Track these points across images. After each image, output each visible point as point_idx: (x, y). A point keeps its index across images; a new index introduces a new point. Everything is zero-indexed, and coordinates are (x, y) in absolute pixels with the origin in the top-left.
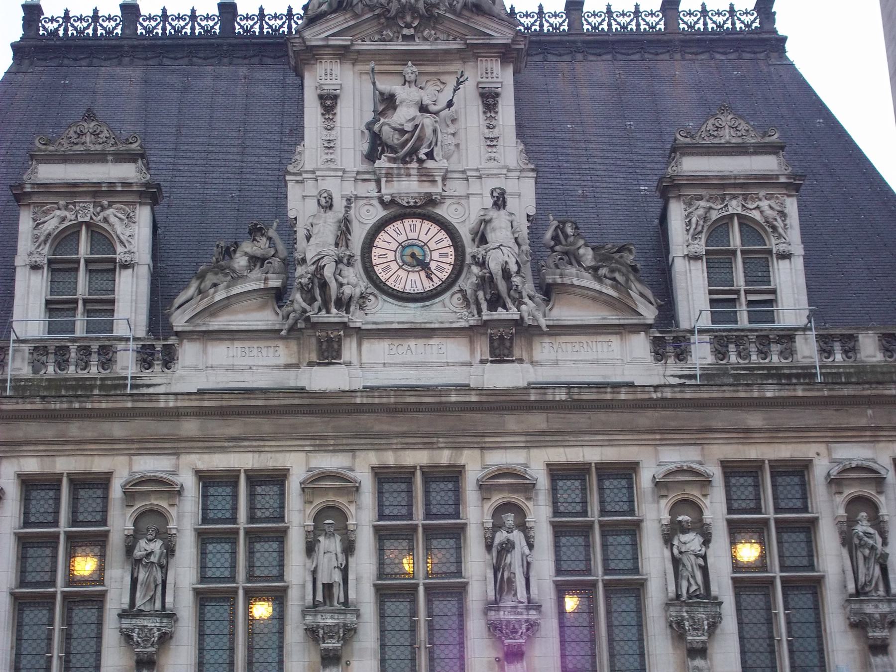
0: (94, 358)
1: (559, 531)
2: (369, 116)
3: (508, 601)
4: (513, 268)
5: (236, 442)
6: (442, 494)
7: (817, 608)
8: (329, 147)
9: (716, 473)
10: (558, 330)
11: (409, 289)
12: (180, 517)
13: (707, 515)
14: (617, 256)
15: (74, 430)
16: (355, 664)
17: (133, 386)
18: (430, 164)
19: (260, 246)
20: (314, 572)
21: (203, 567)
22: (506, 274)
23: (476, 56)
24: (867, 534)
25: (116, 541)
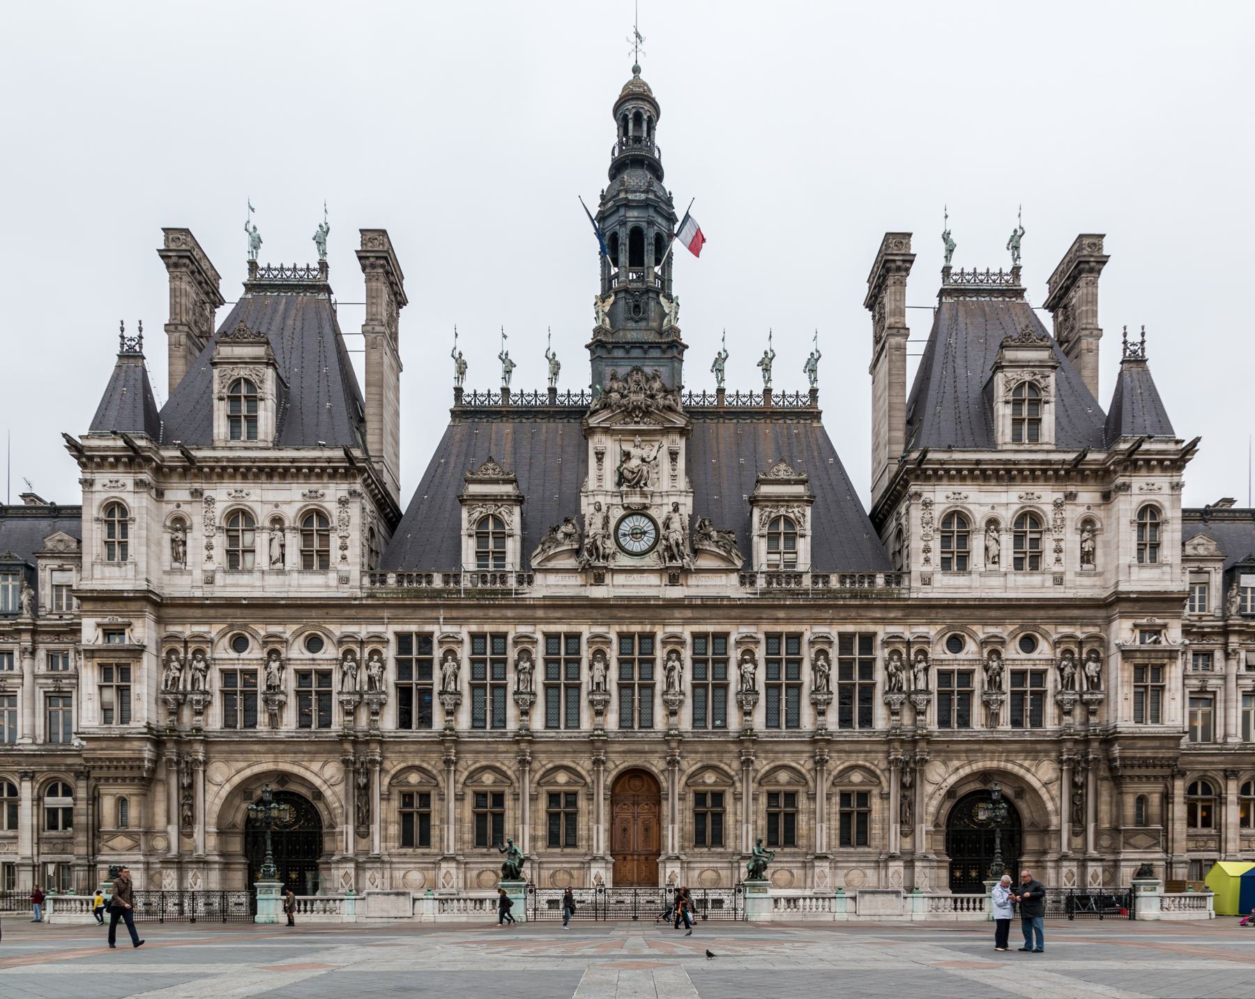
0: (498, 580)
1: (695, 661)
2: (618, 464)
3: (672, 691)
4: (681, 541)
5: (559, 620)
6: (647, 646)
7: (799, 696)
8: (600, 478)
9: (762, 637)
10: (699, 571)
11: (634, 550)
12: (537, 652)
13: (757, 656)
14: (727, 536)
15: (491, 613)
16: (609, 715)
17: (516, 594)
18: (645, 489)
20: (592, 678)
21: (547, 673)
22: (677, 545)
23: (668, 433)
24: (823, 666)
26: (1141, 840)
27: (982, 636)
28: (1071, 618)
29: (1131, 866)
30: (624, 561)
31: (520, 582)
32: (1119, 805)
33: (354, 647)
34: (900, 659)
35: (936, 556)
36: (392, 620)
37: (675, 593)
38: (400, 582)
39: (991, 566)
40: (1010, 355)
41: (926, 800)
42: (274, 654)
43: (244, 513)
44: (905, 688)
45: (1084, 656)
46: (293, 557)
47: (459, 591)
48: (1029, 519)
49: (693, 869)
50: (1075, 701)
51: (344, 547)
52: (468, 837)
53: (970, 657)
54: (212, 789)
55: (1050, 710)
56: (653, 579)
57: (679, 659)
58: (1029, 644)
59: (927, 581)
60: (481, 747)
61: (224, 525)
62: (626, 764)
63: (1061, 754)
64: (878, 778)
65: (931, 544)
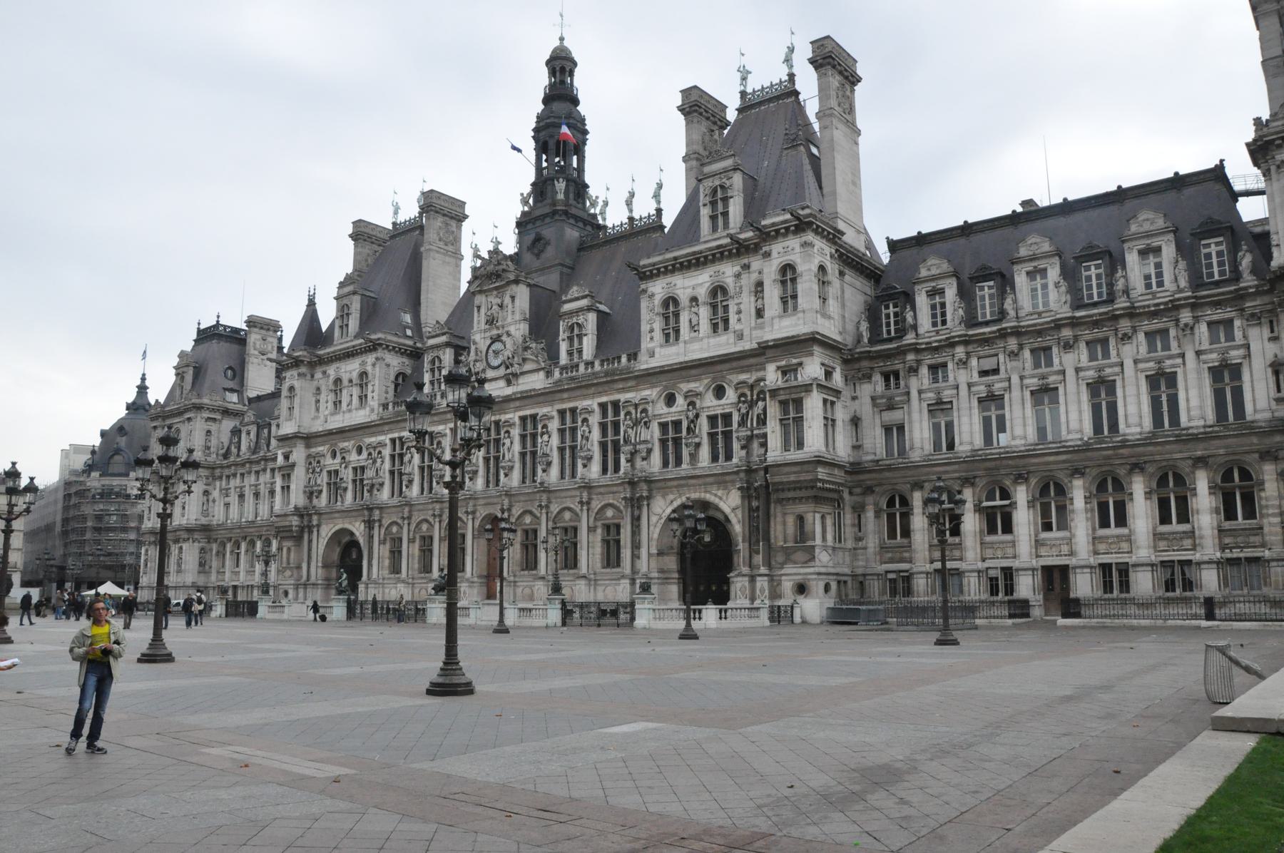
4: (511, 356)
9: (555, 414)
10: (523, 373)
22: (509, 358)
24: (584, 431)
26: (799, 556)
27: (685, 390)
28: (747, 366)
29: (790, 580)
30: (490, 374)
31: (442, 397)
32: (784, 523)
33: (372, 451)
34: (631, 419)
35: (658, 335)
36: (391, 431)
37: (509, 391)
38: (394, 407)
39: (693, 334)
40: (707, 169)
41: (651, 528)
42: (343, 458)
44: (633, 441)
45: (755, 397)
46: (355, 400)
48: (718, 291)
49: (518, 586)
50: (748, 436)
51: (373, 392)
52: (416, 566)
53: (679, 409)
54: (321, 540)
56: (502, 383)
57: (509, 437)
58: (720, 392)
59: (652, 355)
60: (421, 507)
61: (333, 388)
62: (485, 513)
64: (622, 512)
65: (654, 325)
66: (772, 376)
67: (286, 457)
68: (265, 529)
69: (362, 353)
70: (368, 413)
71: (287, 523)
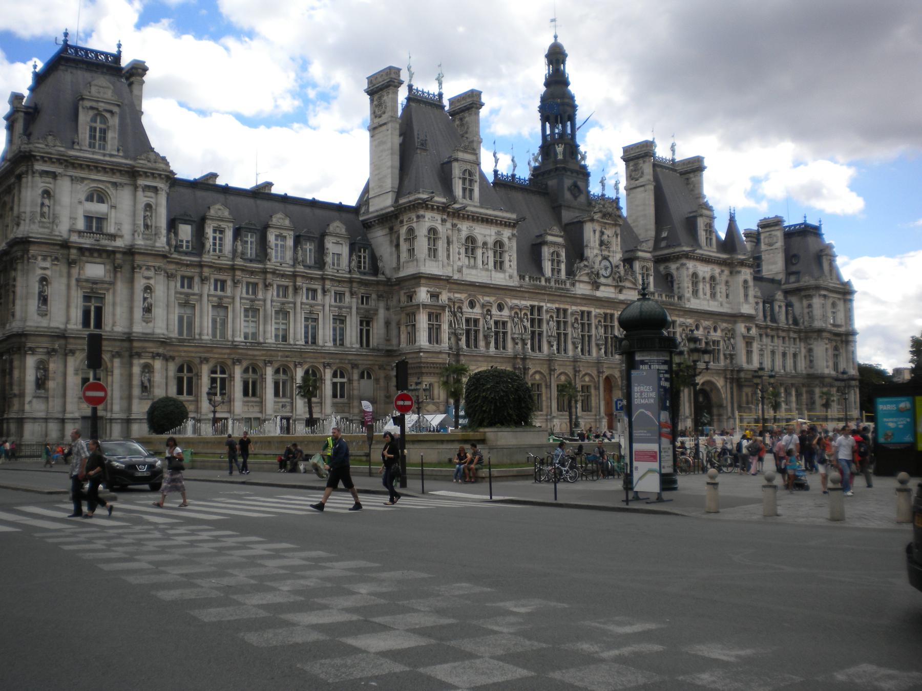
5: (585, 305)
15: (563, 299)
19: (586, 263)
25: (569, 323)
32: (740, 396)
35: (691, 292)
36: (530, 299)
37: (621, 297)
38: (530, 280)
43: (471, 237)
46: (491, 263)
47: (551, 288)
48: (713, 278)
55: (722, 357)
56: (612, 290)
59: (689, 300)
60: (561, 363)
63: (726, 375)
66: (741, 328)
67: (432, 296)
68: (280, 354)
69: (501, 224)
70: (507, 278)
71: (440, 361)
